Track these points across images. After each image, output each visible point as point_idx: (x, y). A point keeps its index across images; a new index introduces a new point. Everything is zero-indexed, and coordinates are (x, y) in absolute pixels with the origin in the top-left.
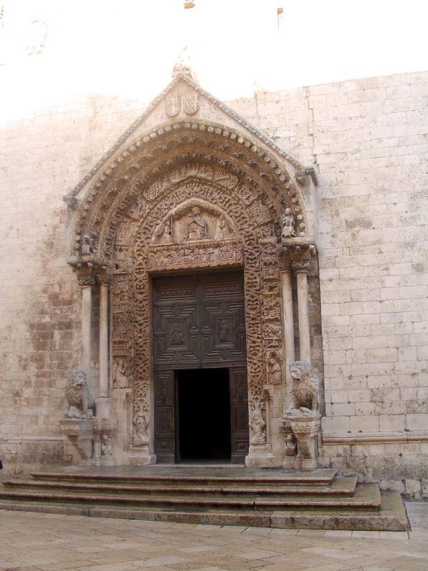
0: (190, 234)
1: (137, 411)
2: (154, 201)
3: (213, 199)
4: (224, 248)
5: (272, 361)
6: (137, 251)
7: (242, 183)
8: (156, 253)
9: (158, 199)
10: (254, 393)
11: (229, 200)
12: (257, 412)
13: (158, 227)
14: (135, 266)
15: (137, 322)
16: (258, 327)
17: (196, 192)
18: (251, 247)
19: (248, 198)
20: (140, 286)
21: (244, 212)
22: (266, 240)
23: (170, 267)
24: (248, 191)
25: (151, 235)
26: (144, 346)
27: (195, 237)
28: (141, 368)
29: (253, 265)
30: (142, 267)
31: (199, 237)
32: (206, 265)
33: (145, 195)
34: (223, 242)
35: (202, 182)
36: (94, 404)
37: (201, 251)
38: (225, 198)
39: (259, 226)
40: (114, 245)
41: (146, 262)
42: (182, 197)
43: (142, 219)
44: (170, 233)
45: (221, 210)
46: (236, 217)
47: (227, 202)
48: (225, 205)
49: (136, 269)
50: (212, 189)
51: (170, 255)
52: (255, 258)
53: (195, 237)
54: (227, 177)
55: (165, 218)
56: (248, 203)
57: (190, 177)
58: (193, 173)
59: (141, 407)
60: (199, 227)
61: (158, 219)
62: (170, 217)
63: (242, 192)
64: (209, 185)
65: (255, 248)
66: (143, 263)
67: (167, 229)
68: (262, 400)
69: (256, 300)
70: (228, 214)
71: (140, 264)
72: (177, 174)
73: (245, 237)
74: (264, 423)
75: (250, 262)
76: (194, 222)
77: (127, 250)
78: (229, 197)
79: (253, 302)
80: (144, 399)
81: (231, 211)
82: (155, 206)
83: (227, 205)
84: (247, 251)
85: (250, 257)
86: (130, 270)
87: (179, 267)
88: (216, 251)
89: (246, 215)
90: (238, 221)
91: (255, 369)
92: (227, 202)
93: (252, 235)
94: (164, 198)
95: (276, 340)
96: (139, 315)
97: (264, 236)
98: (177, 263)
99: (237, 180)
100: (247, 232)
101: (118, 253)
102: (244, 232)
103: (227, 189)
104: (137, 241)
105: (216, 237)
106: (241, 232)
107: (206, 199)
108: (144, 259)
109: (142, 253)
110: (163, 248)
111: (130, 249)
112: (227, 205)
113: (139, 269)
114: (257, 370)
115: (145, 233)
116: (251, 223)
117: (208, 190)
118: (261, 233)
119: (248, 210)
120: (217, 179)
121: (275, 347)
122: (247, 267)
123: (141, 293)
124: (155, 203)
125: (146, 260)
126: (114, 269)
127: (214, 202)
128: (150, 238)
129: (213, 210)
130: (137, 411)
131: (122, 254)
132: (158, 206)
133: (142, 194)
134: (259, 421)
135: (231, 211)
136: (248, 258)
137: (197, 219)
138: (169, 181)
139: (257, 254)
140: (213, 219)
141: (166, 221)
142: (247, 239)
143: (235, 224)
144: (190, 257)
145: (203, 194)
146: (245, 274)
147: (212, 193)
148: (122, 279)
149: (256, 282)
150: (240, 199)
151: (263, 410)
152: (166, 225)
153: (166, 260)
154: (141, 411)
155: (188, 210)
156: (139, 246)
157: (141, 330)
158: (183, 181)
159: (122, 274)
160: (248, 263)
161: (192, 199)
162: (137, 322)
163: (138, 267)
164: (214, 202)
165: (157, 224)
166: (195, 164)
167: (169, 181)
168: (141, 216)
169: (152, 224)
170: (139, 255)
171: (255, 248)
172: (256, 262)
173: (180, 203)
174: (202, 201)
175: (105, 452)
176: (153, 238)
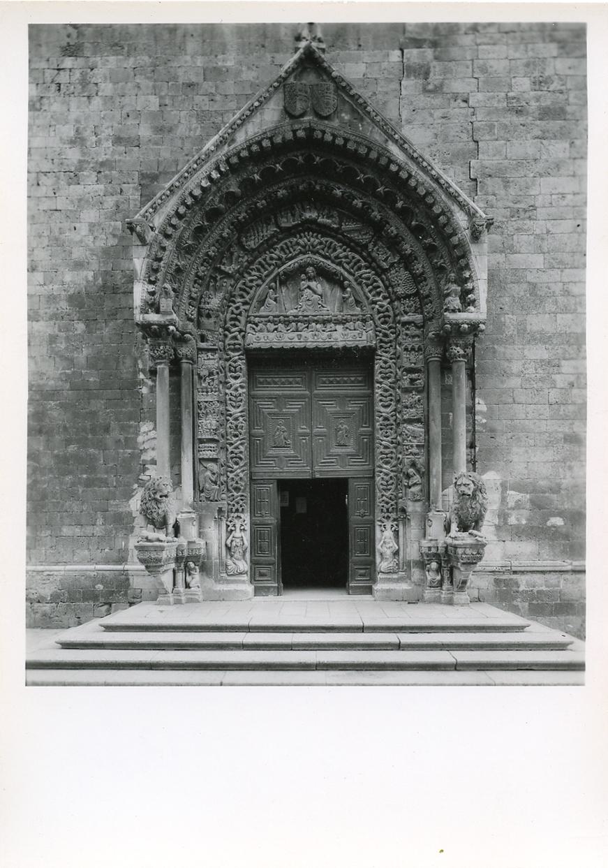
1: (232, 531)
5: (411, 471)
8: (257, 325)
10: (385, 510)
12: (389, 533)
15: (231, 415)
16: (391, 429)
18: (386, 326)
20: (235, 368)
22: (405, 318)
23: (277, 345)
26: (240, 447)
28: (237, 475)
32: (327, 345)
35: (323, 230)
36: (177, 521)
37: (319, 326)
45: (346, 274)
46: (367, 286)
47: (355, 264)
51: (276, 329)
52: (391, 342)
58: (310, 215)
59: (238, 526)
63: (378, 250)
65: (390, 328)
68: (394, 520)
69: (391, 395)
70: (356, 280)
74: (397, 548)
76: (309, 287)
79: (386, 397)
80: (242, 515)
82: (256, 258)
83: (355, 268)
84: (380, 332)
88: (340, 327)
91: (387, 482)
93: (387, 310)
95: (417, 446)
96: (234, 407)
97: (406, 313)
102: (377, 306)
104: (229, 307)
110: (266, 319)
112: (355, 268)
114: (391, 482)
118: (402, 308)
121: (416, 454)
122: (379, 352)
123: (236, 378)
130: (232, 531)
131: (212, 320)
134: (391, 545)
135: (360, 276)
136: (381, 340)
146: (376, 362)
147: (335, 250)
148: (211, 357)
149: (391, 372)
151: (396, 533)
152: (270, 288)
154: (238, 530)
155: (302, 269)
156: (233, 313)
157: (236, 426)
160: (381, 347)
162: (231, 415)
175: (191, 585)
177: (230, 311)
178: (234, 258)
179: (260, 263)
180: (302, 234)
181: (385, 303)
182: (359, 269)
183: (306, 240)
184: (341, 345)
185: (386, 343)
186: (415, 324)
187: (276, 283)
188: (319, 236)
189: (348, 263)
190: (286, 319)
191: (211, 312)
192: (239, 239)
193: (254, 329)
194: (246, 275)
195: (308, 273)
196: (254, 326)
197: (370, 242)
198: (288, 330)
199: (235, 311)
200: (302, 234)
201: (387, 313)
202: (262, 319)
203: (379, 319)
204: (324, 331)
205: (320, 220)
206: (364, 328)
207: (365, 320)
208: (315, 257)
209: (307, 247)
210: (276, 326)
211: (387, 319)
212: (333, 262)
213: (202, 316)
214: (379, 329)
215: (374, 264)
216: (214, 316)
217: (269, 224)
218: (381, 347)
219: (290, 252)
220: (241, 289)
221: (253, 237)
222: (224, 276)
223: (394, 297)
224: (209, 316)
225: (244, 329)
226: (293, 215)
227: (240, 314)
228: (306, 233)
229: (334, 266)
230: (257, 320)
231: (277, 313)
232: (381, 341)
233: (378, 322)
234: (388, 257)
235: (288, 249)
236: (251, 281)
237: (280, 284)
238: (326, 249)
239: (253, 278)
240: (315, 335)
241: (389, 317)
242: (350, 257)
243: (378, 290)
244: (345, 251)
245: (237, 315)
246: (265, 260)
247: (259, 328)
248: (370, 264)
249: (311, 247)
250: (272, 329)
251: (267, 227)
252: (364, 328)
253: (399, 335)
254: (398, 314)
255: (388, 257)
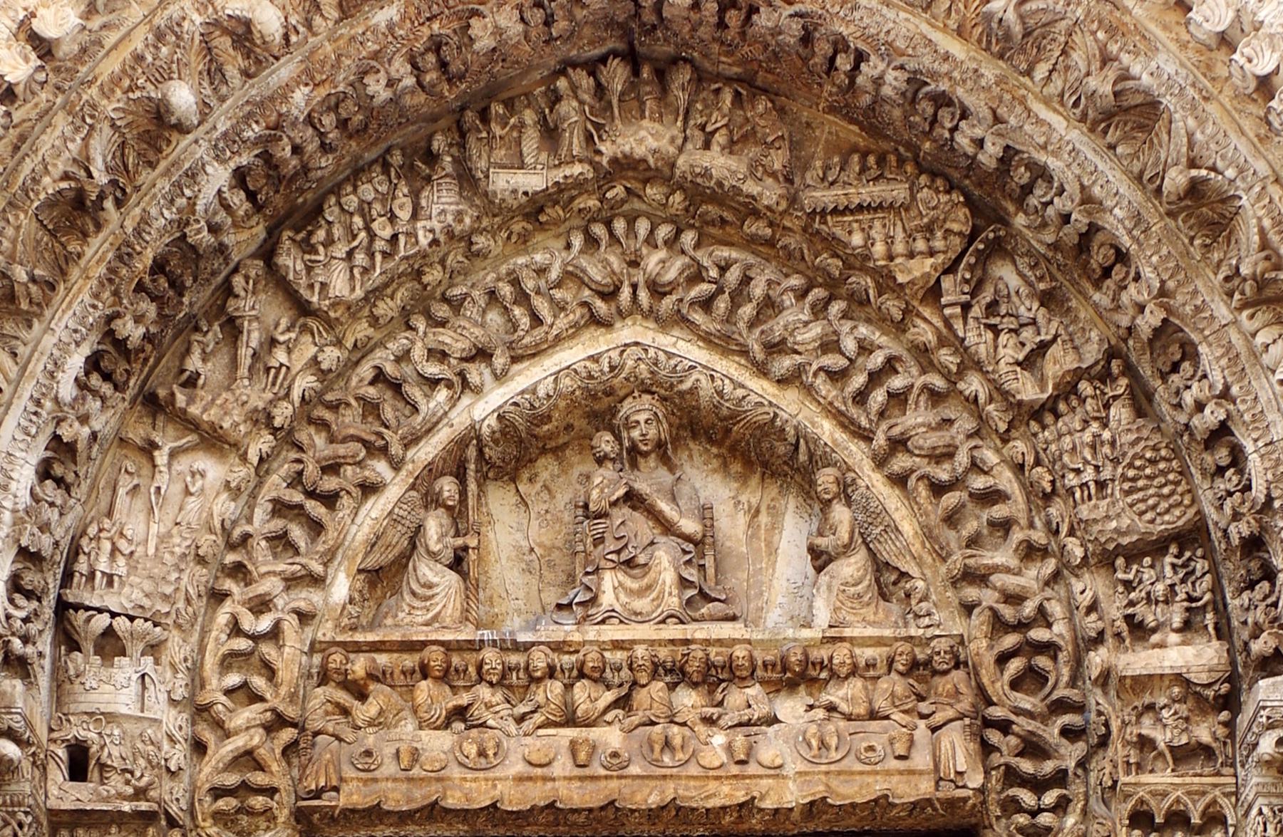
0: (609, 580)
2: (352, 310)
3: (776, 348)
4: (845, 694)
6: (229, 661)
7: (998, 249)
9: (386, 308)
11: (890, 366)
13: (376, 508)
14: (210, 771)
17: (657, 290)
18: (1026, 701)
19: (1031, 361)
21: (990, 457)
22: (1138, 661)
24: (1027, 308)
25: (328, 558)
27: (641, 604)
29: (1045, 819)
30: (259, 779)
31: (673, 602)
32: (727, 794)
33: (290, 261)
34: (841, 654)
37: (688, 699)
38: (865, 348)
39: (1105, 559)
40: (63, 607)
41: (290, 750)
42: (559, 307)
43: (262, 443)
44: (457, 563)
45: (827, 430)
46: (938, 489)
47: (875, 378)
48: (861, 398)
49: (218, 792)
50: (770, 273)
51: (460, 713)
52: (1060, 778)
53: (641, 604)
54: (898, 192)
55: (427, 451)
56: (1028, 390)
57: (625, 166)
60: (672, 541)
61: (384, 450)
62: (461, 443)
63: (992, 308)
64: (751, 243)
65: (1061, 706)
66: (270, 751)
67: (435, 525)
70: (880, 462)
71: (248, 759)
72: (531, 142)
73: (999, 625)
75: (1027, 797)
76: (632, 499)
77: (154, 649)
78: (886, 345)
81: (899, 444)
83: (878, 397)
84: (1004, 727)
85: (1026, 766)
86: (173, 795)
87: (537, 795)
88: (791, 708)
89: (1006, 480)
90: (952, 519)
92: (875, 378)
93: (1041, 616)
94: (421, 305)
97: (1138, 630)
98: (519, 768)
99: (960, 221)
100: (1014, 599)
101: (85, 663)
102: (988, 597)
103: (886, 281)
105: (773, 617)
106: (971, 593)
107: (722, 343)
108: (277, 722)
109: (259, 682)
111: (178, 648)
112: (878, 397)
113: (246, 788)
115: (281, 542)
116: (1039, 537)
117: (746, 280)
118: (1114, 609)
119: (1019, 446)
120: (826, 197)
124: (362, 330)
125: (287, 735)
126: (58, 775)
127: (784, 364)
128: (317, 581)
129: (770, 429)
131: (126, 669)
132: (383, 358)
133: (267, 253)
137: (651, 479)
138: (467, 180)
139: (1071, 754)
140: (752, 496)
141: (432, 471)
142: (1010, 641)
143: (928, 534)
144: (611, 737)
145: (706, 304)
147: (769, 306)
150: (970, 363)
152: (432, 501)
153: (437, 743)
156: (235, 629)
158: (559, 194)
159: (118, 818)
160: (1012, 806)
161: (627, 332)
163: (232, 779)
164: (784, 364)
165: (369, 489)
166: (661, 75)
167: (467, 180)
168: (262, 419)
169: (330, 484)
170: (250, 695)
171: (1061, 706)
172: (1061, 807)
173: (536, 353)
174: (695, 352)
176: (341, 587)
177: (222, 617)
178: (245, 355)
179: (379, 377)
180: (599, 230)
181: (1031, 577)
182: (899, 399)
183: (616, 263)
184: (792, 795)
185: (1038, 785)
186: (1188, 682)
187: (461, 476)
188: (688, 238)
189: (838, 376)
190: (514, 659)
191: (121, 624)
192: (267, 253)
193: (345, 712)
194: (302, 436)
195: (629, 426)
196: (343, 697)
197: (951, 269)
198: (520, 719)
199: (248, 622)
200: (599, 230)
201: (1039, 634)
202: (382, 659)
203: (1003, 659)
204: (709, 721)
205: (694, 160)
206: (924, 707)
207: (928, 663)
208: (665, 341)
209: (626, 293)
210: (464, 699)
211: (1042, 662)
212: (762, 370)
213: (74, 646)
214: (997, 712)
215: (974, 384)
216: (136, 648)
217: (428, 179)
218: (1012, 806)
219: (537, 320)
220: (280, 508)
221: (340, 250)
222: (192, 438)
223: (1076, 550)
224: (110, 645)
225: (291, 712)
226: (551, 134)
227: (275, 634)
228: (620, 226)
229: (761, 388)
230: (359, 666)
231: (466, 633)
232: (1012, 776)
233: (998, 686)
234: (1043, 347)
235: (522, 298)
236: (332, 468)
237: (482, 480)
238: (722, 304)
239: (342, 450)
240: (667, 744)
241: (1049, 648)
242: (850, 345)
243: (999, 511)
244: (819, 310)
245: (255, 638)
246: (403, 357)
247: (370, 709)
248: (952, 379)
249: (643, 296)
250: (440, 711)
251: (415, 195)
252: (924, 707)
253: (1104, 742)
254: (1099, 639)
255: (1043, 347)
